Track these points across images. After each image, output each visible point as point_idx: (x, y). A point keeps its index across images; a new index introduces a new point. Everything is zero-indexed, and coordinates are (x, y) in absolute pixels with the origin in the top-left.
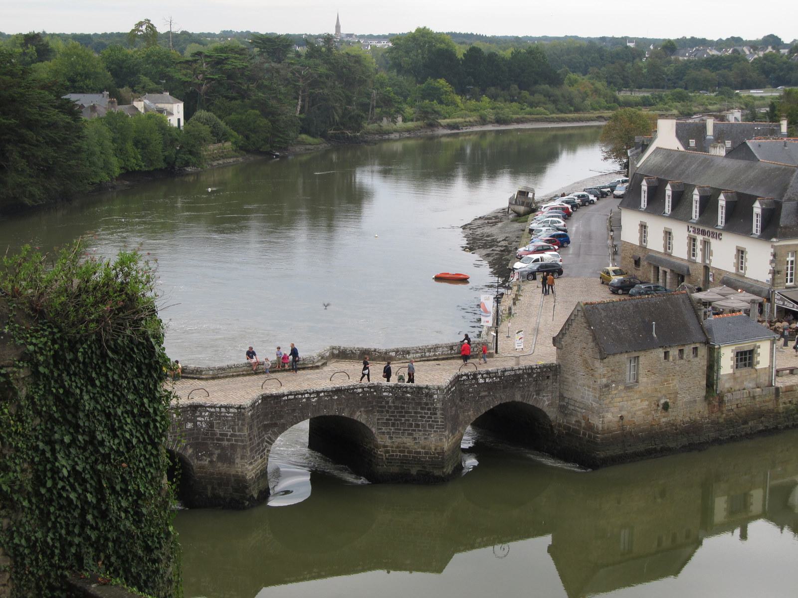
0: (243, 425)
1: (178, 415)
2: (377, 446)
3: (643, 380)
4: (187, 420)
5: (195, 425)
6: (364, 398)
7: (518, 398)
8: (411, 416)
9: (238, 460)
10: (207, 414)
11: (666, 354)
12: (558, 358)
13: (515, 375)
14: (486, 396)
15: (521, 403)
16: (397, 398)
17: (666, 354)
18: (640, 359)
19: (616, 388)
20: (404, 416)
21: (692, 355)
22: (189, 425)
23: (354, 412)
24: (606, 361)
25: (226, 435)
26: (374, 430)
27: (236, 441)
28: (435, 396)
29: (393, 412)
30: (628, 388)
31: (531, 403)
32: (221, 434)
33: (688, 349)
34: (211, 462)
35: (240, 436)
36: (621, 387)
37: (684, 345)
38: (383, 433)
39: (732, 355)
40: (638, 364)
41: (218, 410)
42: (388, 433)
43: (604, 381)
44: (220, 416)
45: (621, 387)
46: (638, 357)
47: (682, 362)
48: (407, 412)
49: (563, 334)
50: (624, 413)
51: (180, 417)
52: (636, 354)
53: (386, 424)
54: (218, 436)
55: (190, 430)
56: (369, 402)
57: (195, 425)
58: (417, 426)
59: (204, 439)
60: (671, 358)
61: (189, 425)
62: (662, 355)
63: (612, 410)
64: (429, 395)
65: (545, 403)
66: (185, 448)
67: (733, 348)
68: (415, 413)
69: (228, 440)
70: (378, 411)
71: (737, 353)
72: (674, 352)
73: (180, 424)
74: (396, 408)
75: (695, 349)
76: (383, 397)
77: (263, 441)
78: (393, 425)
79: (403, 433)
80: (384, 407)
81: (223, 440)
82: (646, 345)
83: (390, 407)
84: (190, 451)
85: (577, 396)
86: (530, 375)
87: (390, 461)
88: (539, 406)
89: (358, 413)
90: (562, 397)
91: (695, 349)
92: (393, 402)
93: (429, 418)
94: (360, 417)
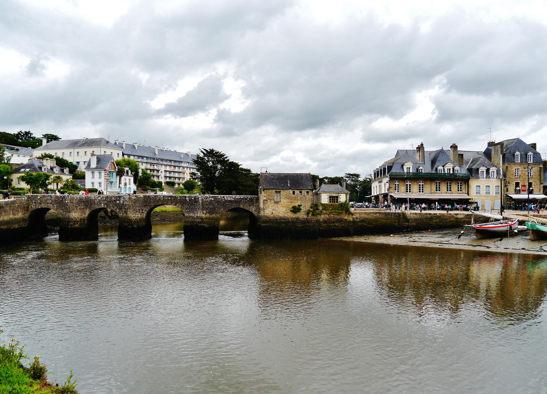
4: (117, 200)
7: (242, 207)
11: (294, 193)
15: (243, 209)
17: (294, 193)
19: (270, 201)
21: (306, 194)
22: (118, 202)
24: (265, 191)
30: (277, 203)
33: (304, 192)
36: (272, 202)
43: (265, 198)
45: (272, 202)
50: (274, 212)
53: (187, 209)
60: (296, 194)
61: (118, 202)
62: (292, 192)
65: (253, 209)
66: (116, 209)
71: (330, 197)
72: (297, 192)
73: (115, 201)
75: (307, 192)
77: (142, 210)
82: (286, 188)
88: (251, 210)
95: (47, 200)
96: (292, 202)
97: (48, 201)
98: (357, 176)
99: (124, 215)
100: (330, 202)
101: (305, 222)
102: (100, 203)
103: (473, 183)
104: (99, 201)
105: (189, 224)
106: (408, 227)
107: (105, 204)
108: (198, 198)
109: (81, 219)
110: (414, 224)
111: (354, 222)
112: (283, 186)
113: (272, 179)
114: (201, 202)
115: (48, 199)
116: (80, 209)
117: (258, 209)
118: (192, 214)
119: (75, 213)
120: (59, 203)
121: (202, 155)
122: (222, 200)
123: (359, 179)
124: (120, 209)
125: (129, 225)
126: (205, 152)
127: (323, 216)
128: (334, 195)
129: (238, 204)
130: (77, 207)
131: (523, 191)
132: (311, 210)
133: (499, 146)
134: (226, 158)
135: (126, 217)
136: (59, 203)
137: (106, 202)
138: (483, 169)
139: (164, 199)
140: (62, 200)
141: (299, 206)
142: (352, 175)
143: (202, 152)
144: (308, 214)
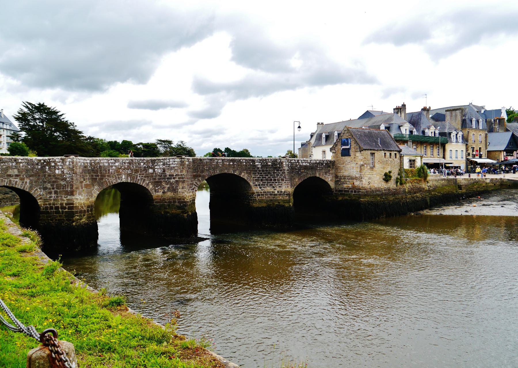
0: (183, 168)
1: (144, 163)
2: (253, 193)
3: (377, 165)
4: (149, 167)
5: (154, 171)
6: (246, 166)
7: (318, 175)
8: (271, 175)
9: (179, 190)
10: (161, 163)
12: (334, 157)
13: (316, 163)
14: (303, 172)
15: (319, 178)
16: (263, 166)
18: (376, 154)
20: (267, 175)
22: (151, 171)
23: (241, 173)
24: (362, 152)
25: (173, 175)
26: (251, 184)
27: (179, 178)
28: (284, 163)
29: (261, 173)
31: (323, 178)
32: (170, 175)
33: (393, 153)
34: (164, 192)
35: (182, 175)
37: (391, 151)
38: (256, 185)
39: (408, 161)
40: (374, 157)
41: (168, 160)
42: (259, 185)
43: (362, 163)
44: (169, 164)
45: (369, 167)
46: (374, 153)
47: (391, 159)
48: (270, 173)
49: (336, 145)
51: (145, 165)
52: (373, 152)
53: (256, 180)
54: (168, 176)
55: (152, 174)
56: (249, 168)
57: (154, 171)
58: (275, 180)
59: (159, 179)
61: (151, 171)
63: (366, 178)
64: (282, 163)
65: (329, 179)
66: (148, 185)
67: (408, 157)
68: (274, 173)
69: (174, 178)
70: (253, 174)
72: (388, 154)
73: (146, 169)
74: (263, 171)
75: (395, 154)
76: (255, 166)
78: (262, 180)
79: (267, 184)
80: (256, 171)
81: (171, 179)
83: (260, 171)
84: (151, 186)
85: (346, 174)
86: (322, 164)
87: (261, 201)
88: (326, 180)
89: (243, 174)
90: (337, 177)
91: (395, 154)
92: (261, 168)
93: (281, 175)
94: (244, 175)
95: (8, 168)
96: (384, 168)
97: (10, 172)
98: (170, 142)
99: (170, 194)
100: (411, 167)
101: (395, 193)
102: (120, 174)
103: (448, 147)
104: (118, 170)
105: (264, 205)
106: (462, 195)
107: (128, 175)
108: (282, 163)
109: (88, 207)
110: (464, 191)
111: (429, 191)
112: (376, 147)
113: (361, 135)
114: (286, 168)
115: (11, 168)
116: (87, 186)
117: (338, 180)
118: (269, 189)
119: (80, 194)
120: (37, 175)
121: (26, 110)
122: (296, 165)
123: (172, 145)
124: (157, 184)
125: (183, 212)
126: (30, 107)
127: (408, 185)
128: (413, 158)
129: (314, 172)
130: (81, 182)
131: (477, 155)
132: (399, 177)
133: (458, 111)
134: (61, 116)
135: (174, 199)
136: (37, 175)
137: (129, 172)
138: (454, 133)
139: (223, 165)
140: (43, 167)
141: (390, 172)
142: (164, 141)
143: (27, 107)
144: (397, 182)
